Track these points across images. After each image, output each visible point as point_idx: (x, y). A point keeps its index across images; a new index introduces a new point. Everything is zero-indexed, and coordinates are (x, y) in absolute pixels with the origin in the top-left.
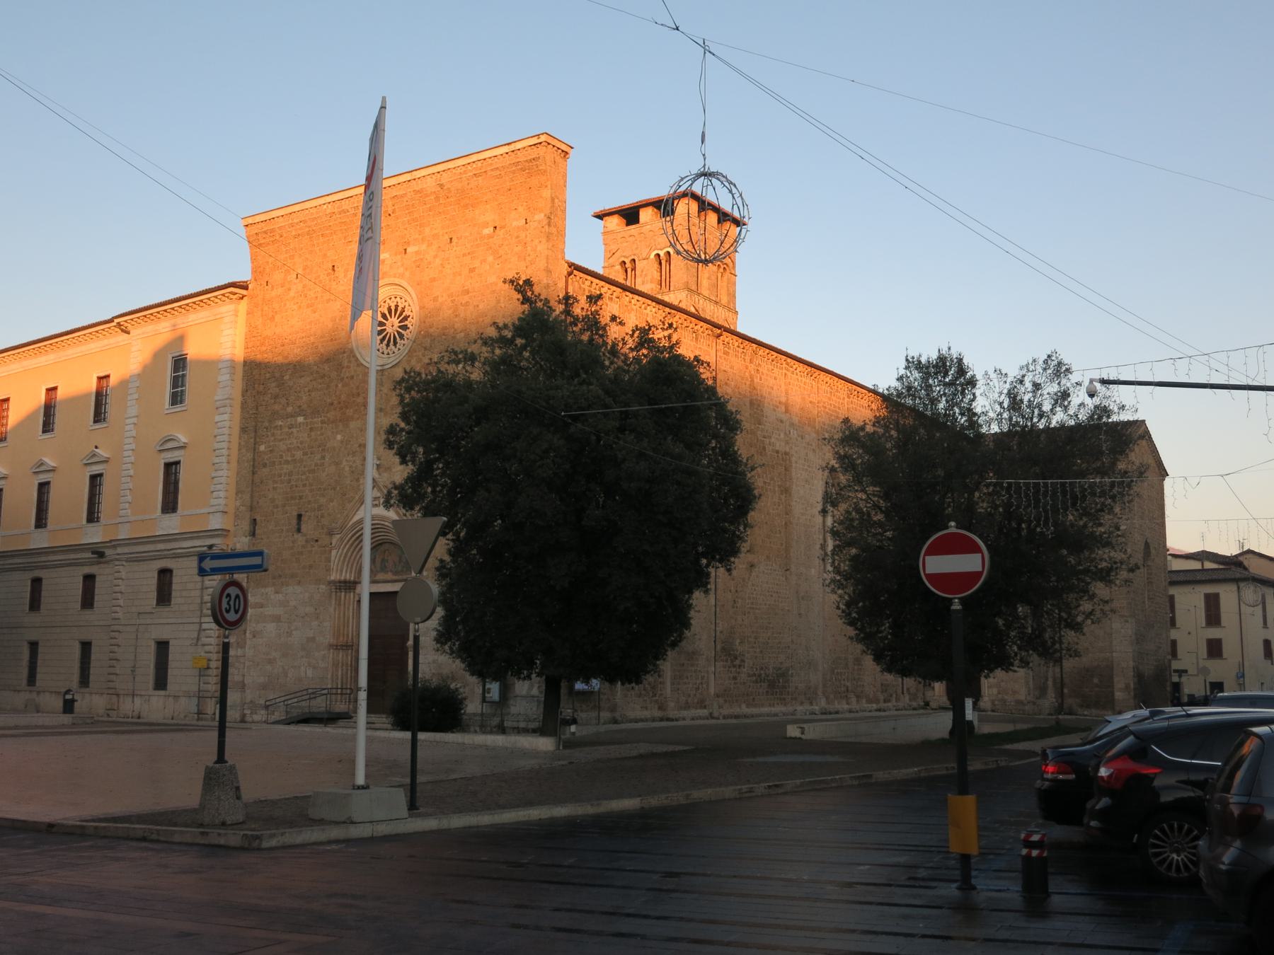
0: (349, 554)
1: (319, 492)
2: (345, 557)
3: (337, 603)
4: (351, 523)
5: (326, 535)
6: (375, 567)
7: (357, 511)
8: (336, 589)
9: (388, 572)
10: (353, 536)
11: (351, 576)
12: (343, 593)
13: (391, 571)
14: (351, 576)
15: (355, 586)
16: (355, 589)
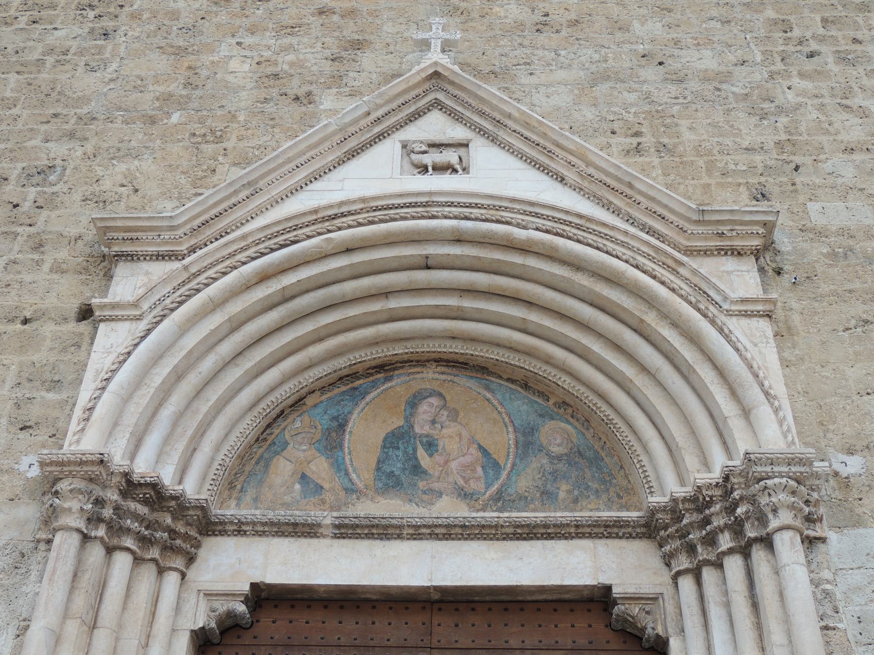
0: (208, 364)
1: (44, 127)
2: (178, 375)
3: (80, 602)
4: (260, 222)
5: (58, 269)
6: (339, 467)
7: (315, 177)
8: (94, 520)
9: (440, 494)
10: (264, 277)
11: (182, 474)
12: (122, 561)
13: (465, 495)
14: (182, 474)
15: (198, 546)
16: (191, 560)
